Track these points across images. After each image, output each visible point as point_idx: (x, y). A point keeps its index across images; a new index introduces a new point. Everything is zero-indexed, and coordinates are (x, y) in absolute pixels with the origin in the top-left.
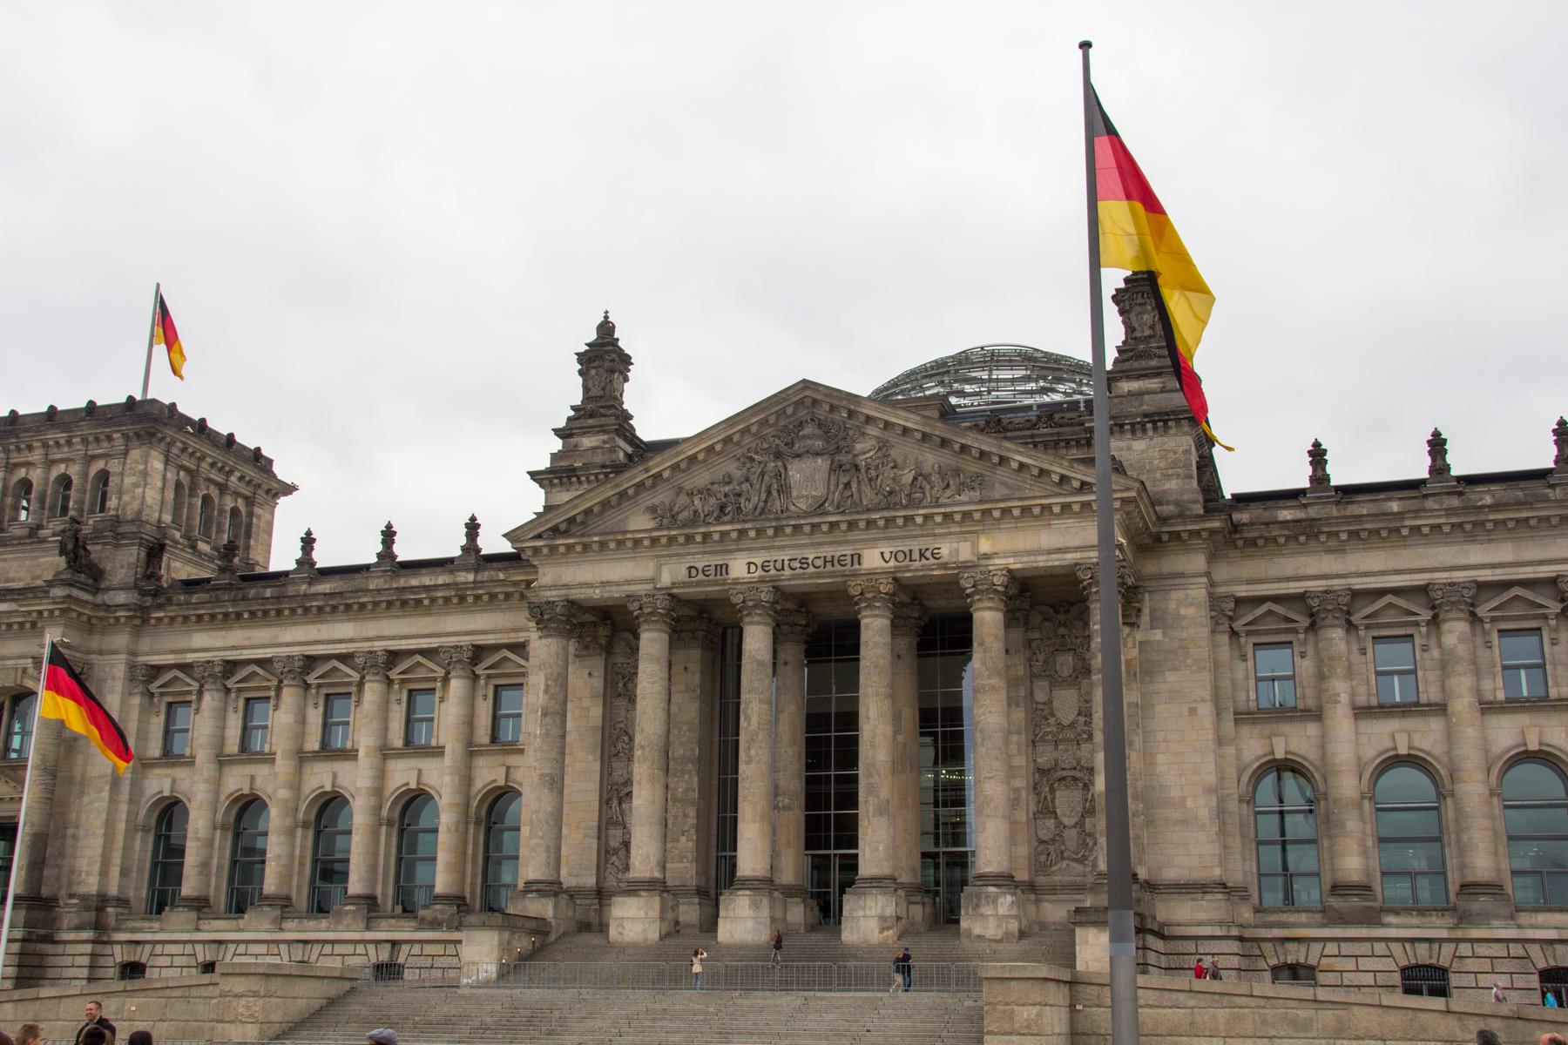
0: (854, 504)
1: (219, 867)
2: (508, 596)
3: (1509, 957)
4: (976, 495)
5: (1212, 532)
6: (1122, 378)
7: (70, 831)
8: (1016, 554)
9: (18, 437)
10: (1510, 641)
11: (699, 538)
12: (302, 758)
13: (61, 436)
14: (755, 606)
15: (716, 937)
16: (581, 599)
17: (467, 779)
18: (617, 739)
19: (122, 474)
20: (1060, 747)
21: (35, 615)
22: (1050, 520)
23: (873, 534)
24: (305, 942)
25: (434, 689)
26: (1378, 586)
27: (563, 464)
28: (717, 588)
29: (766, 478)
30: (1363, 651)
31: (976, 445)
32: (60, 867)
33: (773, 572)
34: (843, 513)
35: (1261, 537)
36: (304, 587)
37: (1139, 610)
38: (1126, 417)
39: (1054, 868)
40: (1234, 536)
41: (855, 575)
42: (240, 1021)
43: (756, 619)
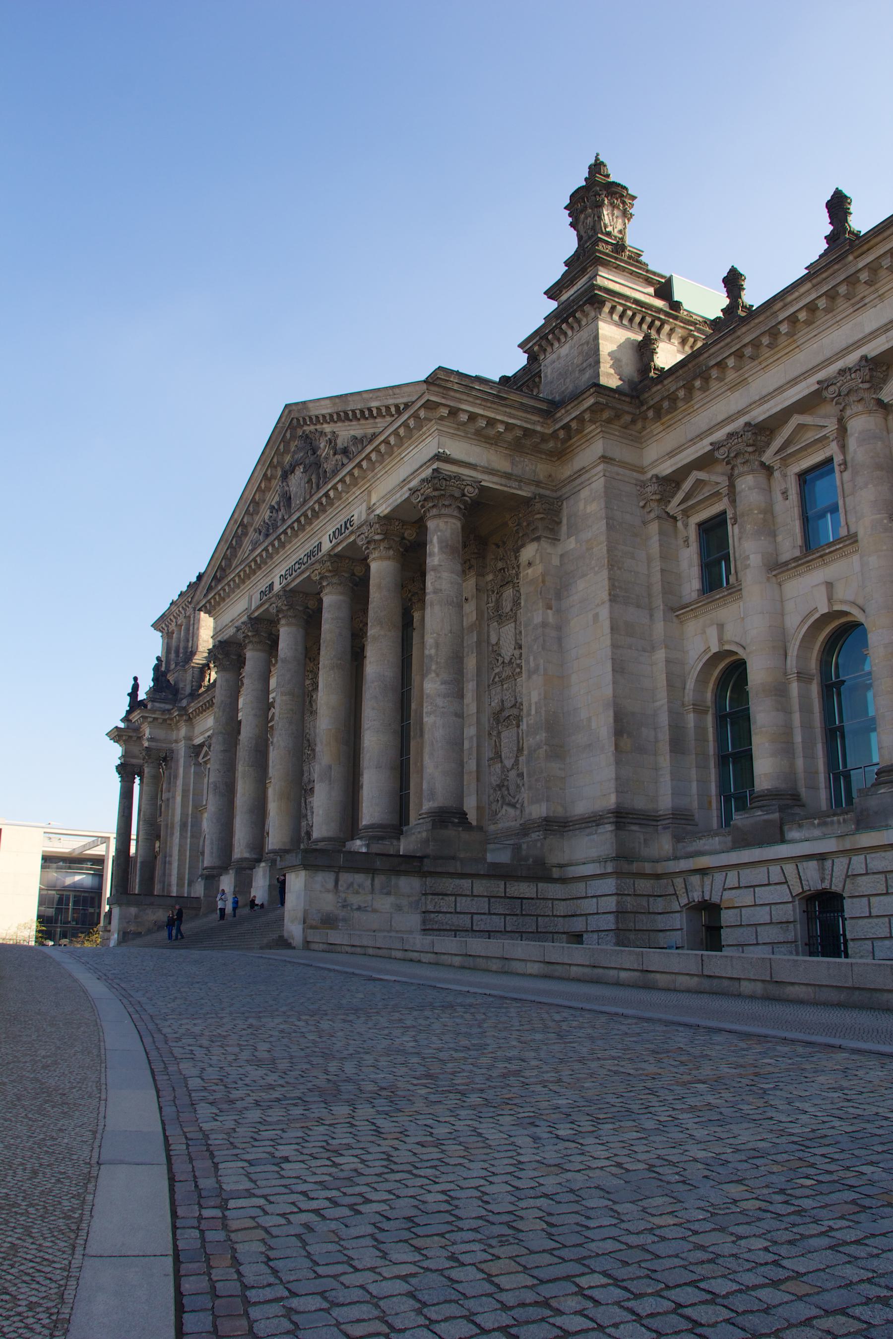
6: (561, 292)
20: (505, 686)
22: (400, 454)
26: (778, 408)
30: (785, 494)
32: (164, 882)
35: (662, 400)
37: (559, 523)
39: (500, 815)
40: (645, 408)
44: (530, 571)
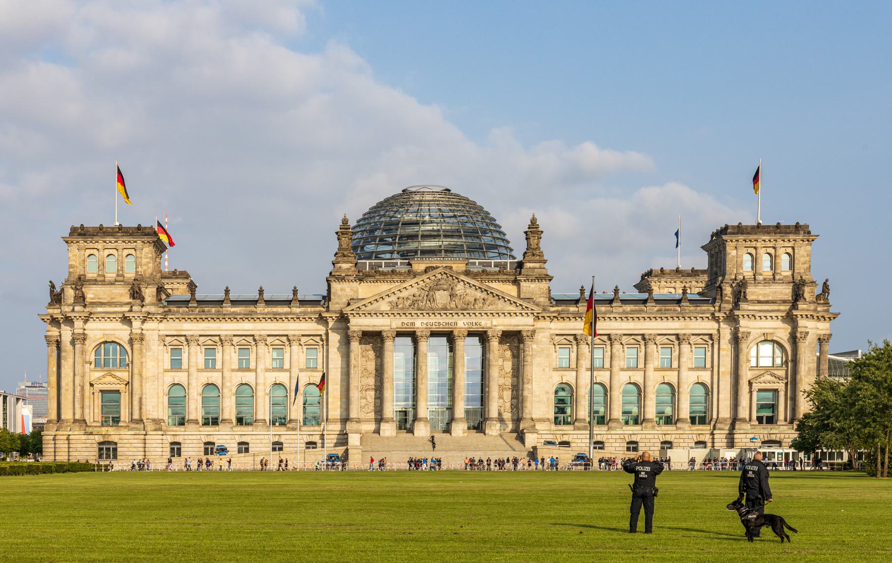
4: (494, 307)
7: (144, 396)
8: (504, 325)
9: (92, 238)
15: (414, 434)
19: (141, 258)
29: (429, 297)
33: (429, 326)
36: (230, 309)
41: (455, 328)
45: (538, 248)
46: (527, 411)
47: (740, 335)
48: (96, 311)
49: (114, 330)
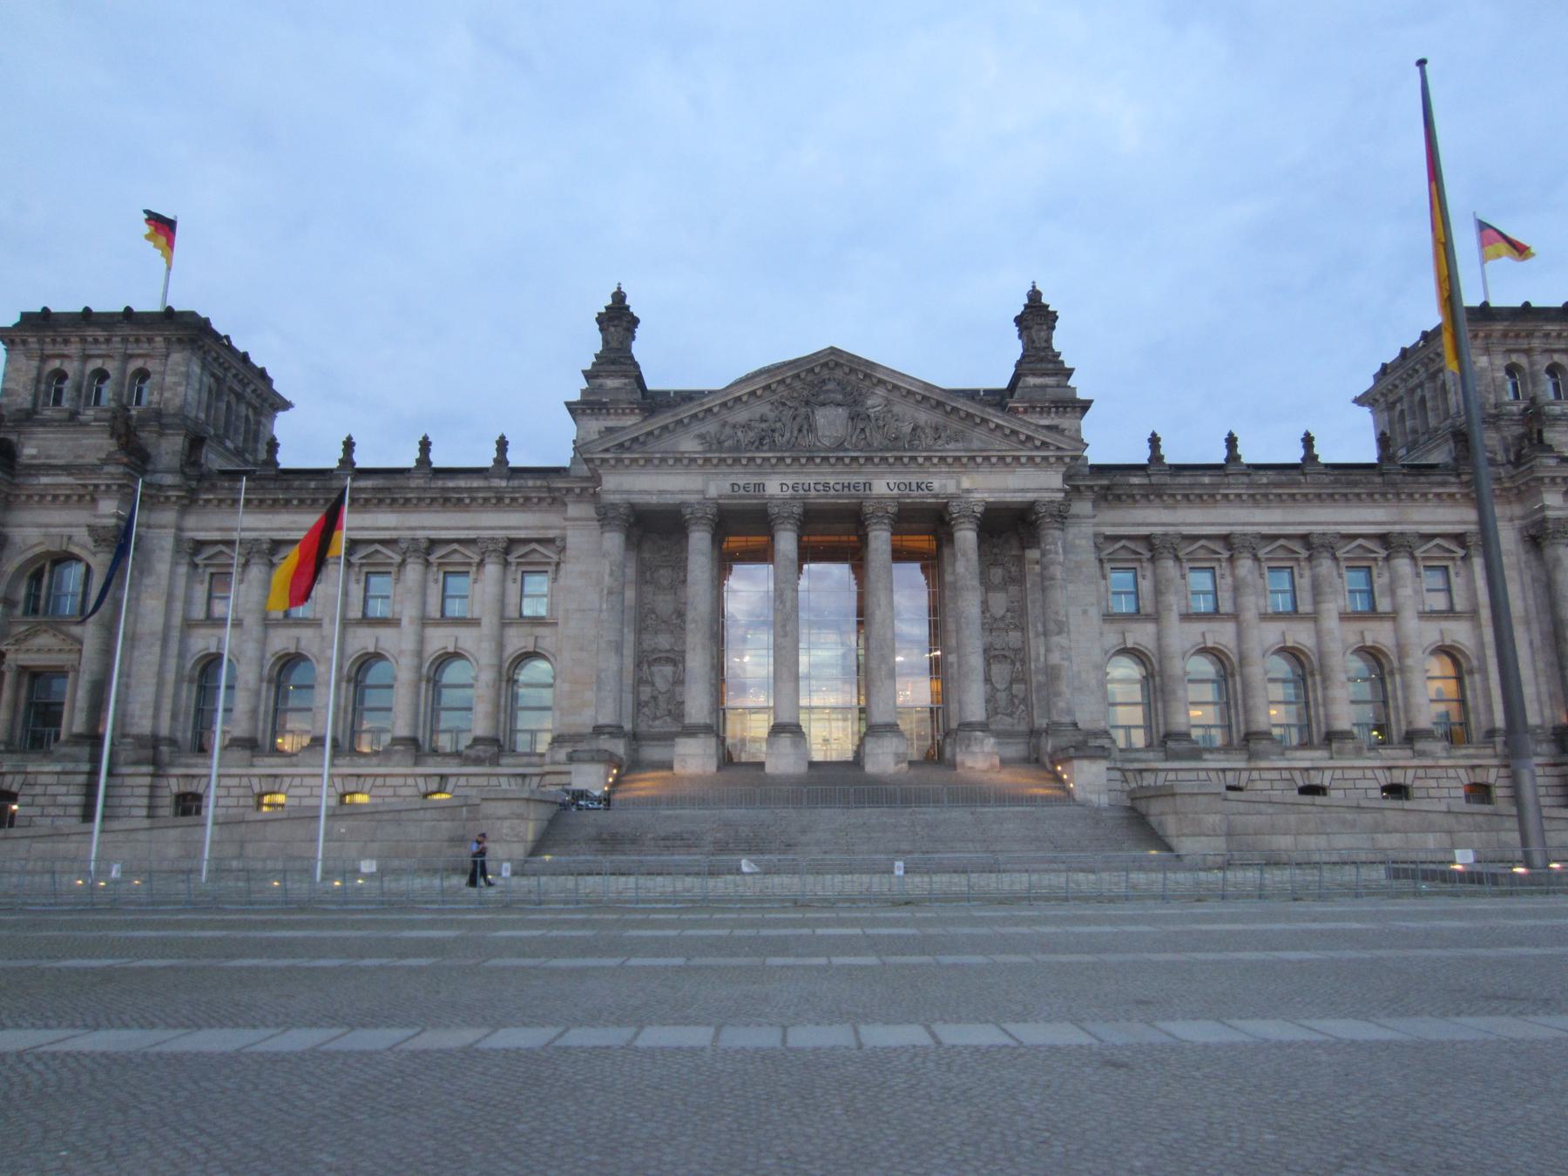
0: (869, 445)
1: (266, 712)
2: (540, 499)
3: (1282, 780)
4: (960, 445)
5: (1102, 487)
8: (990, 491)
9: (55, 331)
10: (1276, 574)
11: (744, 462)
12: (346, 623)
13: (101, 334)
14: (788, 517)
16: (639, 504)
17: (501, 646)
18: (646, 616)
19: (163, 373)
21: (91, 488)
23: (883, 468)
24: (359, 776)
25: (468, 572)
27: (591, 398)
28: (756, 501)
29: (798, 419)
31: (964, 408)
33: (801, 492)
34: (861, 450)
38: (1039, 401)
39: (992, 720)
42: (506, 841)
43: (789, 526)
44: (1037, 568)
45: (1050, 347)
46: (1062, 704)
47: (1550, 526)
48: (36, 482)
49: (71, 526)
